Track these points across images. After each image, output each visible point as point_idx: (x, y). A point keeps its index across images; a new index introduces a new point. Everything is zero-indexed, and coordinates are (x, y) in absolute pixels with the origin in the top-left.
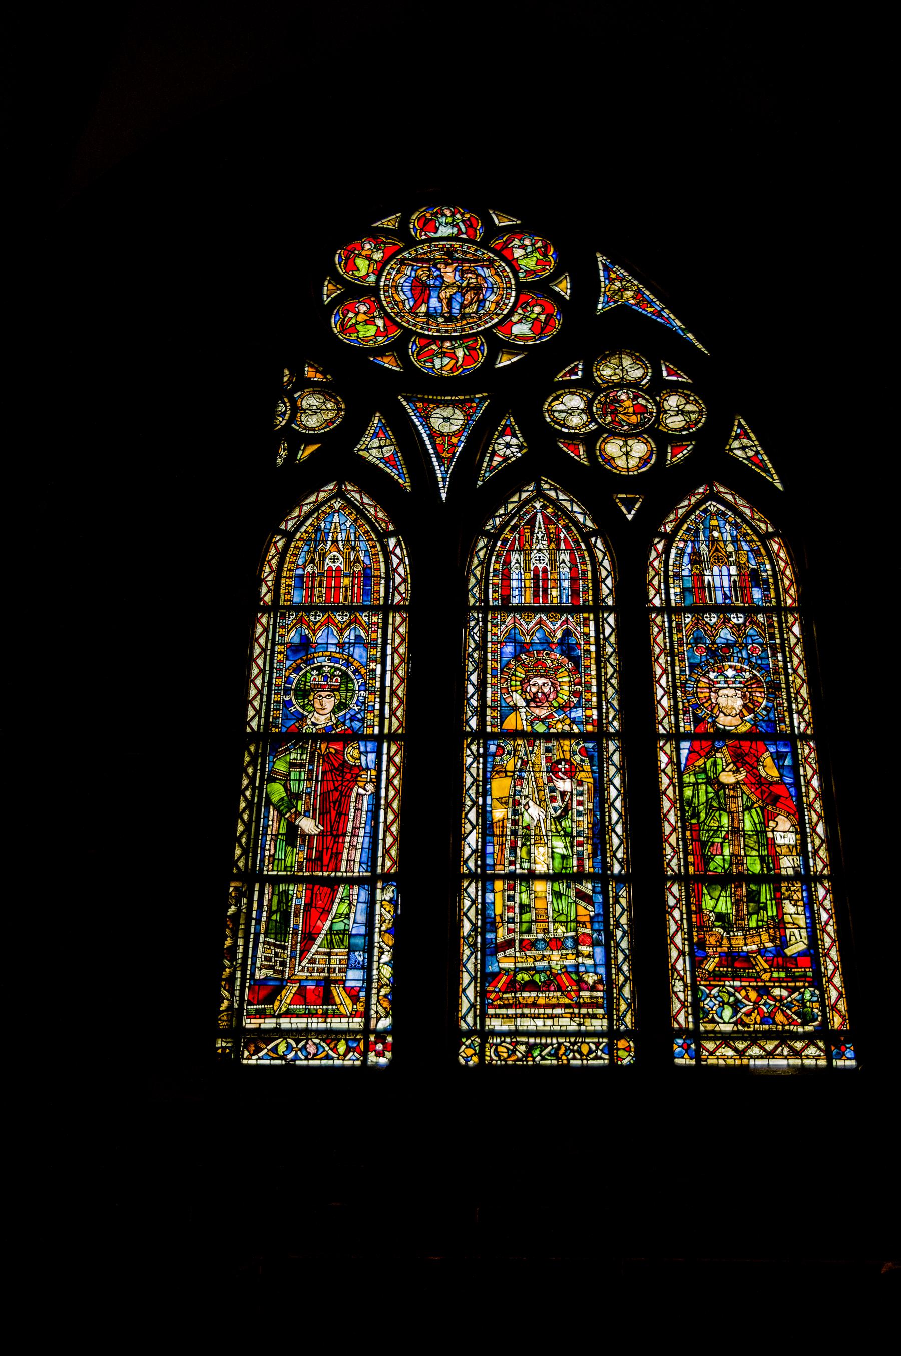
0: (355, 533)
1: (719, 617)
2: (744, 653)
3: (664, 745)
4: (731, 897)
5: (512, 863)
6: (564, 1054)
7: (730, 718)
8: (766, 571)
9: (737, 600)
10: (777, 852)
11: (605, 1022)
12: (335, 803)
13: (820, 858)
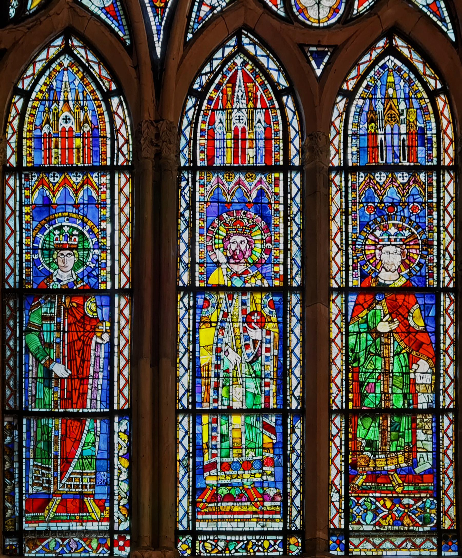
0: (83, 92)
1: (387, 177)
2: (406, 211)
3: (336, 298)
4: (379, 427)
5: (216, 401)
6: (251, 548)
7: (390, 272)
8: (431, 129)
9: (404, 159)
10: (416, 390)
11: (281, 525)
12: (79, 351)
13: (449, 395)
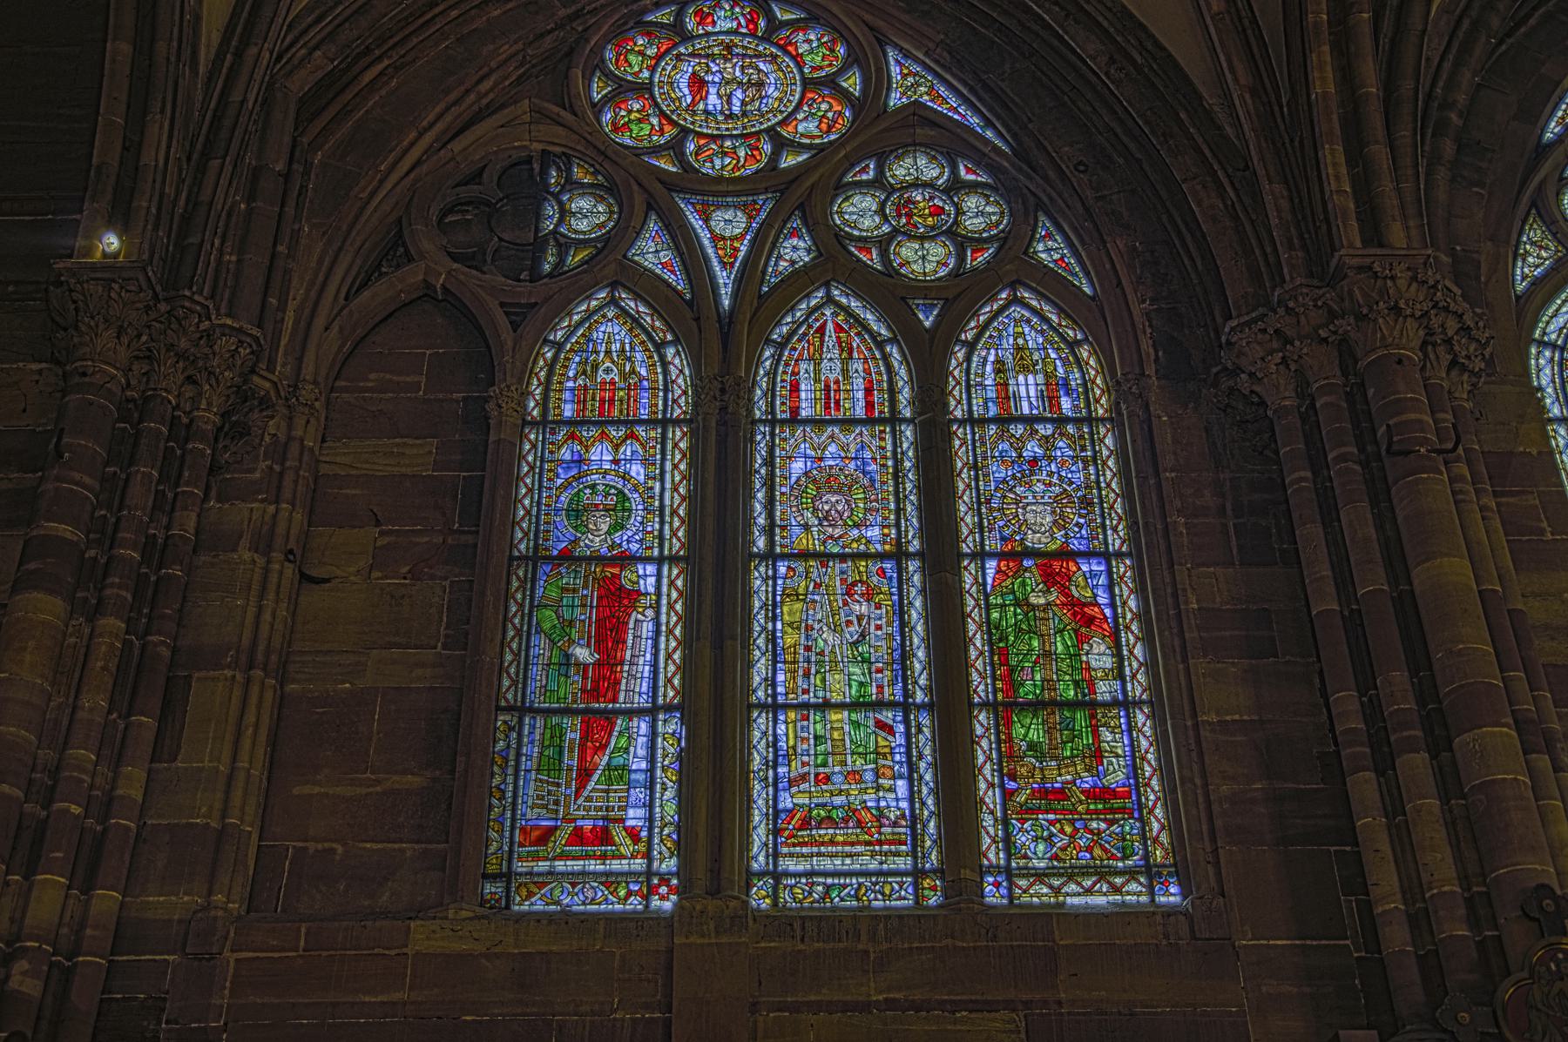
2: (1053, 466)
5: (806, 692)
9: (1045, 410)
